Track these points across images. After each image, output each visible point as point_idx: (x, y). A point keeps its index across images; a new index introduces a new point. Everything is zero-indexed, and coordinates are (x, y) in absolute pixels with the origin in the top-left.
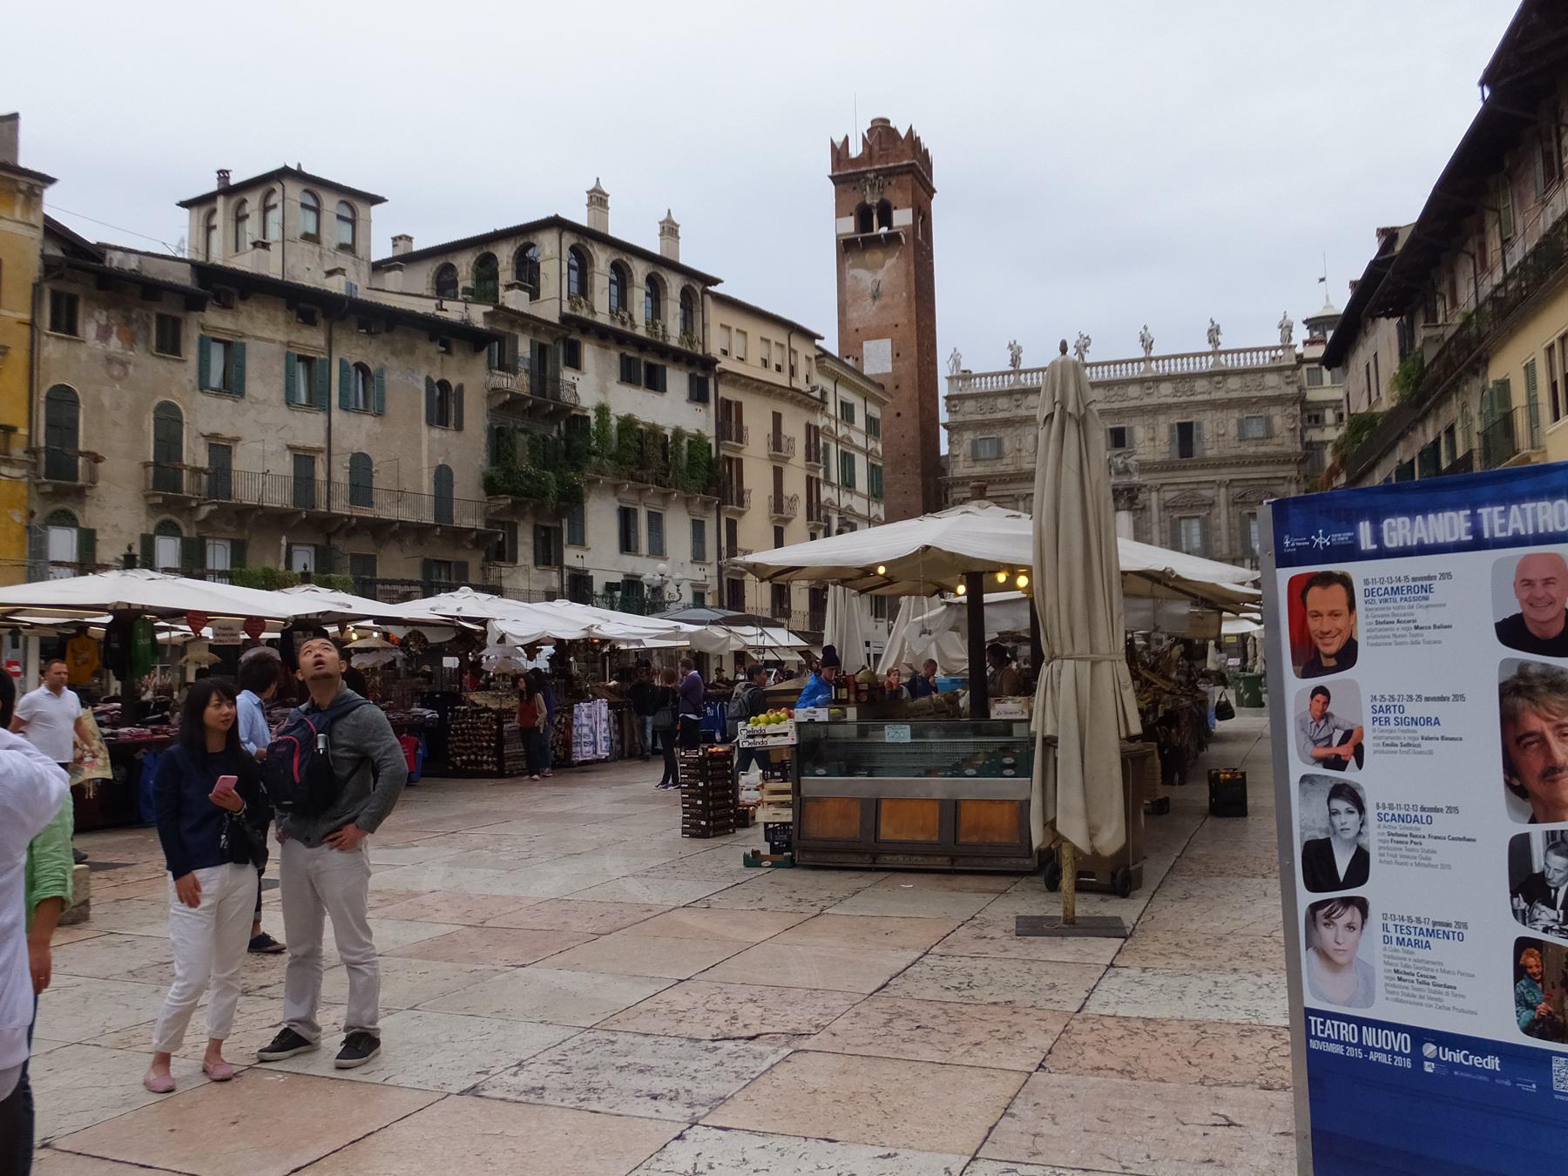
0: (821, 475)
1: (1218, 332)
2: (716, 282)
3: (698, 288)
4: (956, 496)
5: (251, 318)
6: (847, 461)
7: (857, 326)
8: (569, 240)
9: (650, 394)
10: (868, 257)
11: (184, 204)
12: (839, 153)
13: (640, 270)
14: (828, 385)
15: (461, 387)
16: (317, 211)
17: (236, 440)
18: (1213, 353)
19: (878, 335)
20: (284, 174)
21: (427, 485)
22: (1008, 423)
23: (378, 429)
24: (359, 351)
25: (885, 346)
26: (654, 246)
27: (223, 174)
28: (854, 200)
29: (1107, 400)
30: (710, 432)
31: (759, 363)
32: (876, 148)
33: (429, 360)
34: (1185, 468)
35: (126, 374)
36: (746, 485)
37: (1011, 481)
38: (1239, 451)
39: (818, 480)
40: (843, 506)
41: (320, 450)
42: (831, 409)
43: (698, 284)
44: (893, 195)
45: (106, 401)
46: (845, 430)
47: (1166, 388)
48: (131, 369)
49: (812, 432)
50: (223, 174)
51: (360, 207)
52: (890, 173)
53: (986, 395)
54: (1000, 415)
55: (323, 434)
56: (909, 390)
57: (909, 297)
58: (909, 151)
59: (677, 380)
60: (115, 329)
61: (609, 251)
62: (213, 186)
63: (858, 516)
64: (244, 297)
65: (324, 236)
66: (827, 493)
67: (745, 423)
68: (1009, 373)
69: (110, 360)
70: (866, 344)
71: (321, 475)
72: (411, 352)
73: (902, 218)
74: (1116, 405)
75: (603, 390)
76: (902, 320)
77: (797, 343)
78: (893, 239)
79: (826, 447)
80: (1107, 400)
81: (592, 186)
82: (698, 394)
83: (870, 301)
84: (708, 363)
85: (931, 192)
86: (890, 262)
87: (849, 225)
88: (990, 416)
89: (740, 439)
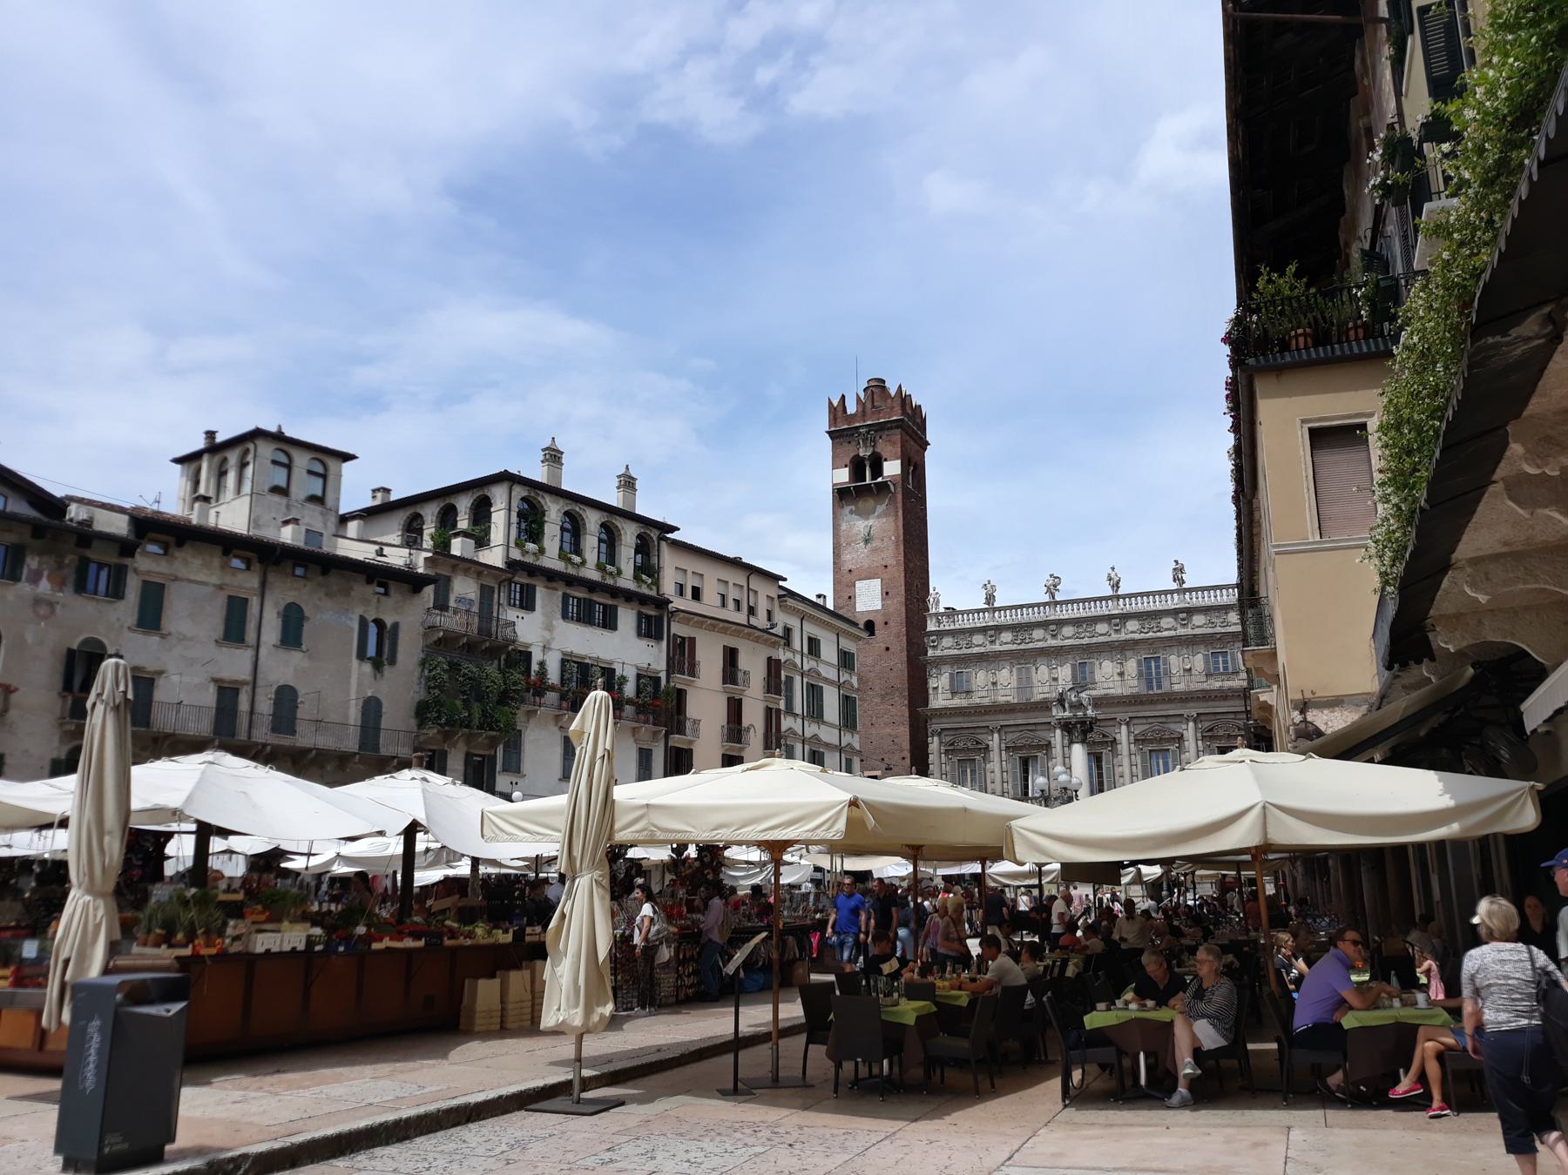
0: (782, 705)
1: (1182, 570)
2: (674, 529)
3: (654, 534)
5: (186, 563)
6: (815, 693)
8: (519, 492)
9: (606, 633)
11: (178, 461)
12: (837, 412)
13: (593, 520)
14: (794, 622)
15: (396, 626)
16: (289, 467)
17: (160, 673)
18: (1177, 591)
20: (257, 434)
21: (354, 714)
23: (306, 663)
24: (293, 593)
25: (876, 584)
26: (613, 498)
27: (211, 435)
28: (849, 452)
29: (1076, 636)
30: (660, 665)
31: (718, 602)
32: (869, 405)
33: (365, 601)
34: (1152, 702)
35: (53, 612)
37: (986, 713)
38: (1205, 686)
39: (778, 711)
40: (807, 735)
41: (244, 683)
42: (796, 644)
43: (654, 534)
44: (883, 447)
45: (30, 638)
46: (813, 664)
47: (1132, 625)
48: (58, 607)
49: (773, 666)
50: (211, 435)
51: (332, 463)
52: (881, 428)
53: (962, 631)
54: (975, 650)
55: (248, 667)
56: (898, 626)
57: (897, 538)
58: (898, 409)
59: (627, 617)
60: (46, 573)
61: (562, 502)
62: (199, 444)
63: (827, 745)
64: (180, 544)
65: (294, 489)
66: (787, 723)
68: (983, 611)
69: (37, 601)
70: (858, 584)
71: (244, 704)
72: (347, 593)
73: (892, 468)
74: (1086, 641)
75: (549, 627)
76: (891, 562)
77: (756, 583)
78: (883, 487)
79: (790, 680)
80: (1076, 636)
81: (547, 443)
82: (650, 629)
84: (662, 603)
85: (924, 444)
87: (843, 476)
88: (965, 651)
89: (692, 673)
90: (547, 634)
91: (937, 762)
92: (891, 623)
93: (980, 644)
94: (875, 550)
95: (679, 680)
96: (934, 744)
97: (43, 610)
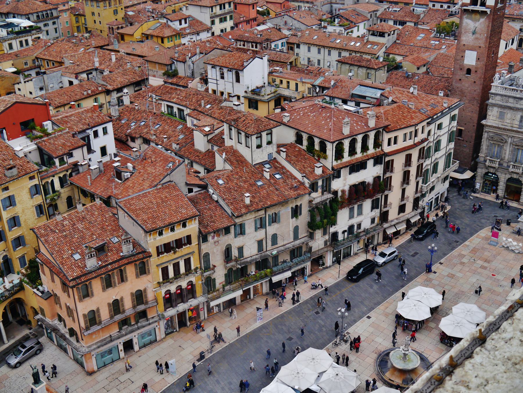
4: (486, 130)
7: (464, 43)
10: (473, 16)
15: (301, 205)
19: (472, 49)
22: (510, 108)
36: (392, 184)
45: (215, 251)
53: (506, 96)
54: (509, 105)
55: (264, 233)
56: (481, 72)
57: (487, 37)
67: (394, 166)
76: (483, 45)
83: (471, 34)
86: (482, 20)
90: (344, 182)
91: (485, 142)
92: (478, 72)
93: (511, 103)
94: (477, 39)
95: (388, 175)
96: (485, 135)
97: (217, 244)
